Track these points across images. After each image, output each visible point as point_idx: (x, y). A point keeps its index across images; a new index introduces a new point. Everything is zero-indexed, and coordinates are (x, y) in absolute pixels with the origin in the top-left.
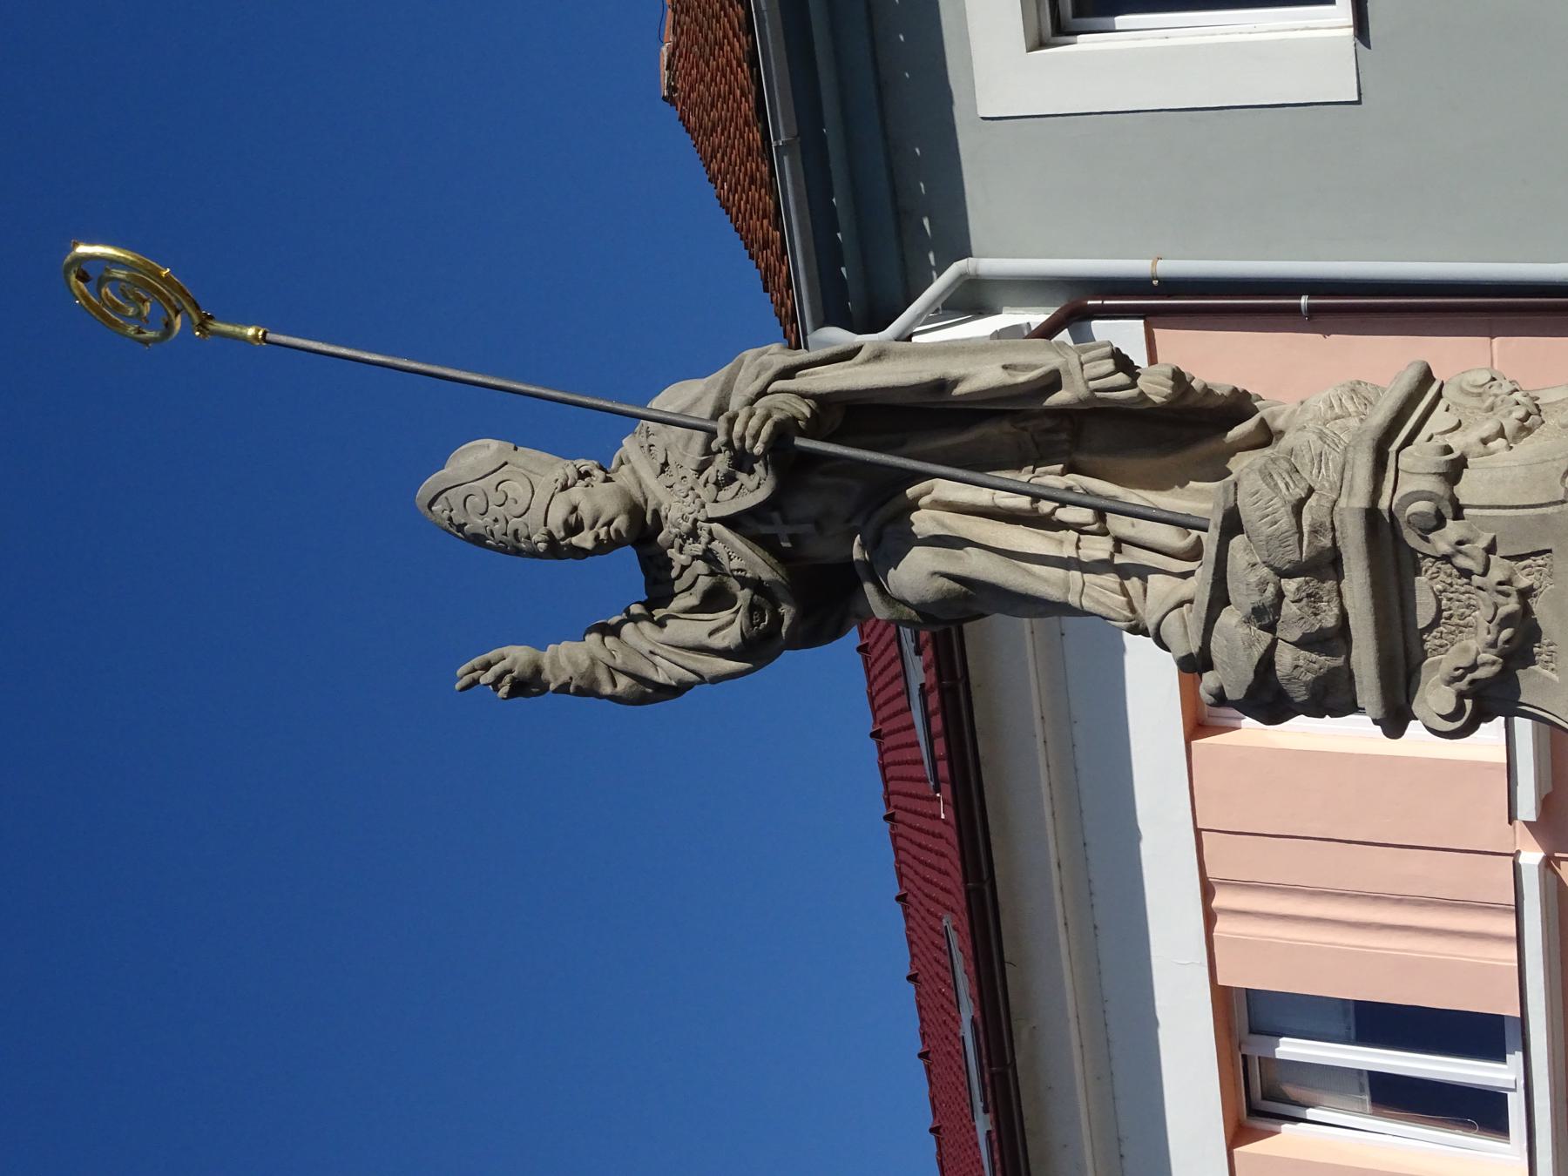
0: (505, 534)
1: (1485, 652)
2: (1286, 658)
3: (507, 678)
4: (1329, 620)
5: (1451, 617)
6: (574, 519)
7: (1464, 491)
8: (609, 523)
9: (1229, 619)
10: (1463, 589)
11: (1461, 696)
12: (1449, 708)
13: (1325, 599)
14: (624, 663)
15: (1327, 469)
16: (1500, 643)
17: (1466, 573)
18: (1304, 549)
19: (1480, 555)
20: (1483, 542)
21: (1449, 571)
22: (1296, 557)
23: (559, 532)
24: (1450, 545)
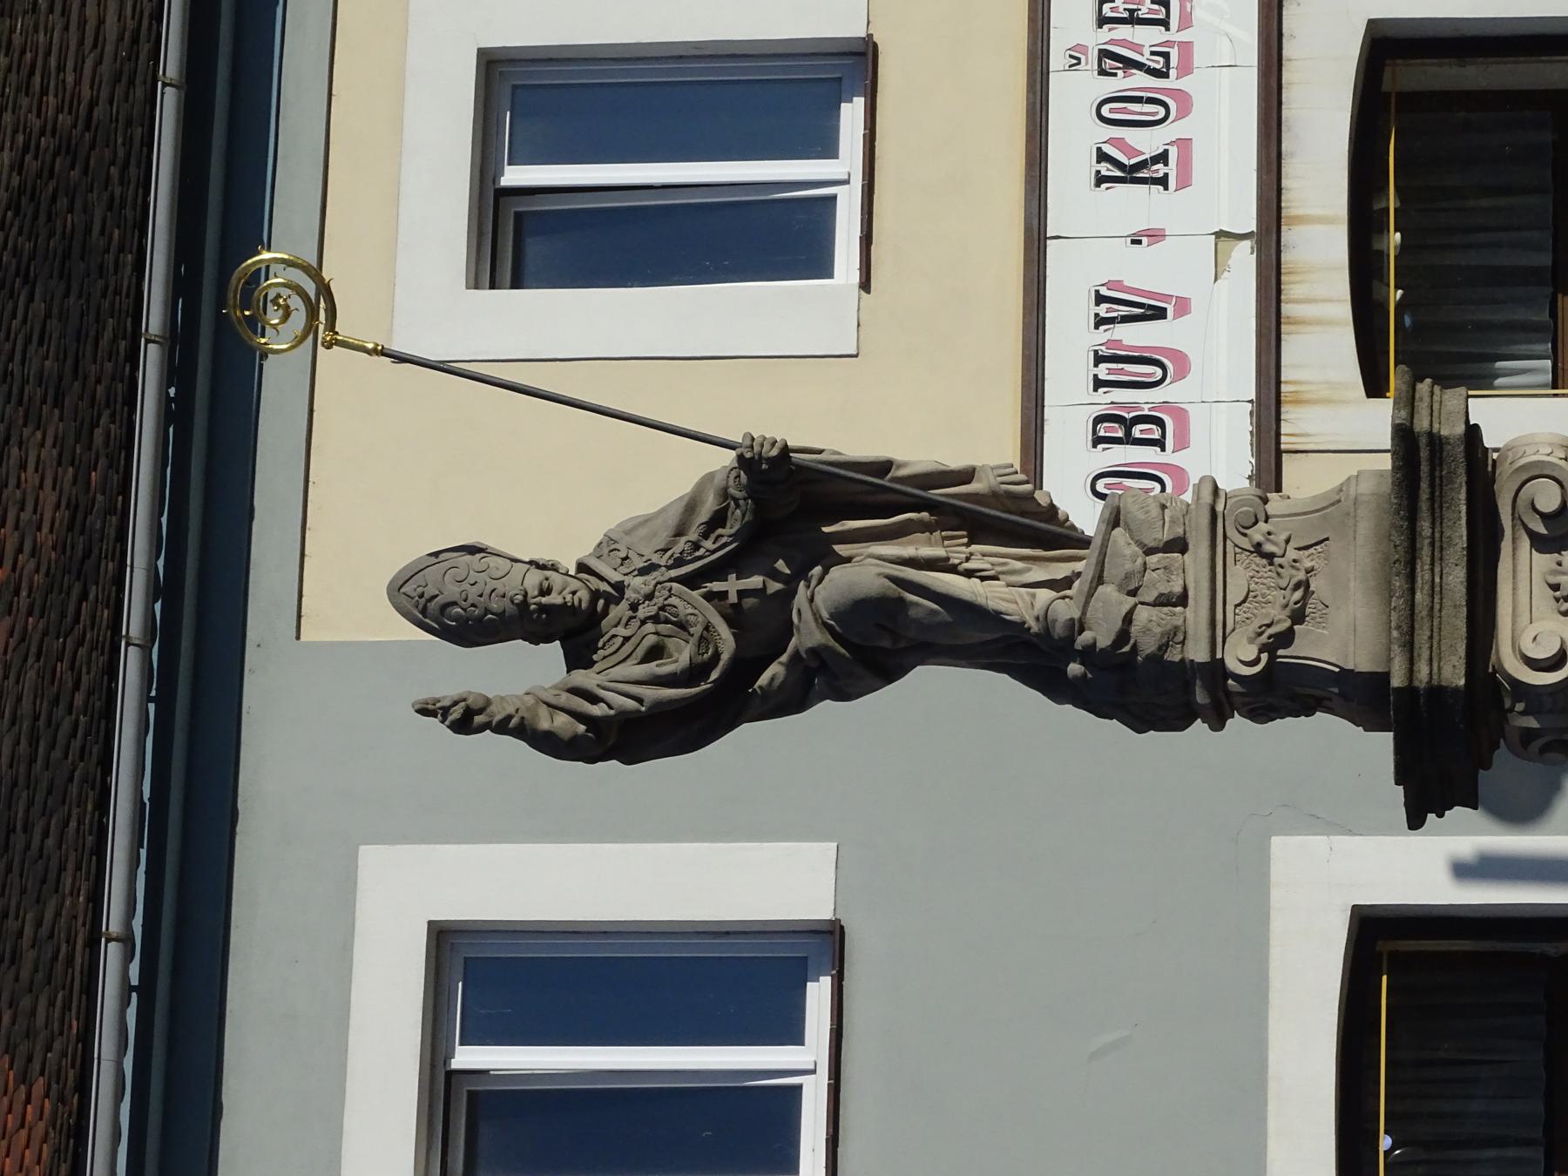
0: (481, 596)
1: (1279, 614)
2: (1143, 615)
3: (463, 704)
4: (1178, 589)
5: (1255, 597)
6: (547, 585)
7: (1271, 508)
8: (574, 593)
9: (1108, 591)
10: (1266, 575)
11: (1261, 651)
12: (1252, 657)
13: (1175, 573)
14: (568, 699)
15: (1176, 504)
16: (1291, 603)
17: (1270, 557)
18: (1165, 532)
19: (1283, 544)
20: (1284, 537)
21: (1258, 562)
22: (1160, 536)
23: (533, 592)
24: (1264, 535)
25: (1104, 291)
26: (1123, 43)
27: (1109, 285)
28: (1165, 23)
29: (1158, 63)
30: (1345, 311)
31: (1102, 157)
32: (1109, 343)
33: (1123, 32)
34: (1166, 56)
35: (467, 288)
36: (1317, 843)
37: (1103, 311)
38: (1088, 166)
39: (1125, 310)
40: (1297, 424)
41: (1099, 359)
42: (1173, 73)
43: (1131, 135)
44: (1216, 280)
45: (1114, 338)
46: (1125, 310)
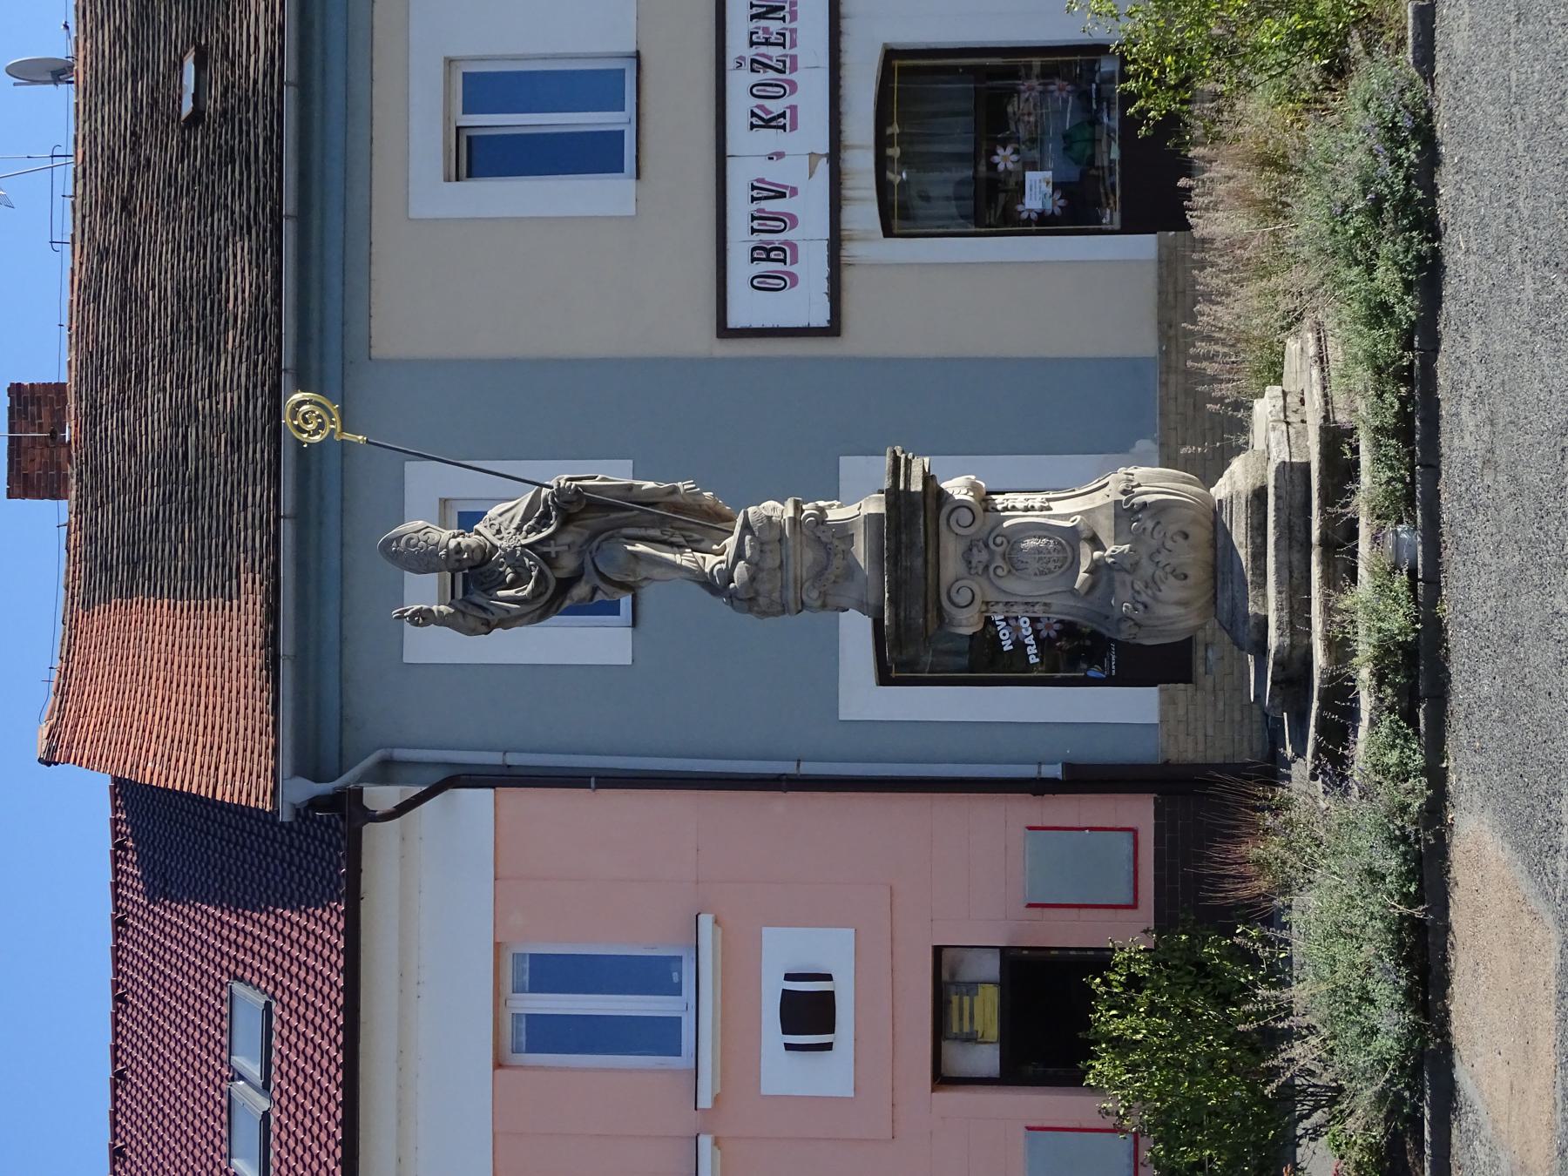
25: (756, 184)
26: (763, 55)
27: (758, 180)
28: (783, 45)
29: (780, 66)
30: (873, 193)
31: (753, 114)
32: (758, 211)
33: (763, 49)
34: (784, 62)
35: (445, 181)
36: (861, 460)
37: (755, 193)
38: (746, 120)
39: (765, 194)
40: (850, 250)
41: (753, 218)
42: (787, 71)
43: (768, 103)
44: (810, 177)
45: (762, 207)
46: (765, 194)
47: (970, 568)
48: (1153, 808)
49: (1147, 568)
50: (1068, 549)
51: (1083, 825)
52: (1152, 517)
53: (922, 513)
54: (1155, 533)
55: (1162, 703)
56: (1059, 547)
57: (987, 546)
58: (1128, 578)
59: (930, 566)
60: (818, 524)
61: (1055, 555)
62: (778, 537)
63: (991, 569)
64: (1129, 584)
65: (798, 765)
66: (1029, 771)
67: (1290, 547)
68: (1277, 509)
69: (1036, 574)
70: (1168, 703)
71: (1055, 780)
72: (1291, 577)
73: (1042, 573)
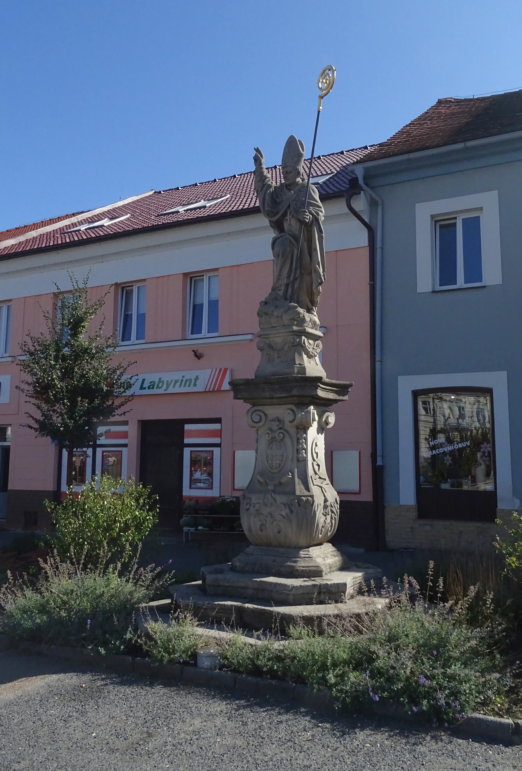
47: (271, 421)
48: (369, 501)
49: (265, 511)
50: (277, 471)
51: (362, 473)
52: (287, 514)
53: (287, 395)
54: (279, 516)
55: (407, 506)
56: (278, 465)
57: (280, 429)
58: (260, 501)
59: (270, 400)
60: (293, 343)
61: (274, 464)
62: (286, 325)
63: (269, 432)
64: (259, 501)
65: (378, 361)
66: (379, 453)
67: (254, 589)
68: (271, 584)
69: (267, 454)
70: (408, 508)
71: (376, 462)
72: (242, 588)
73: (267, 457)
